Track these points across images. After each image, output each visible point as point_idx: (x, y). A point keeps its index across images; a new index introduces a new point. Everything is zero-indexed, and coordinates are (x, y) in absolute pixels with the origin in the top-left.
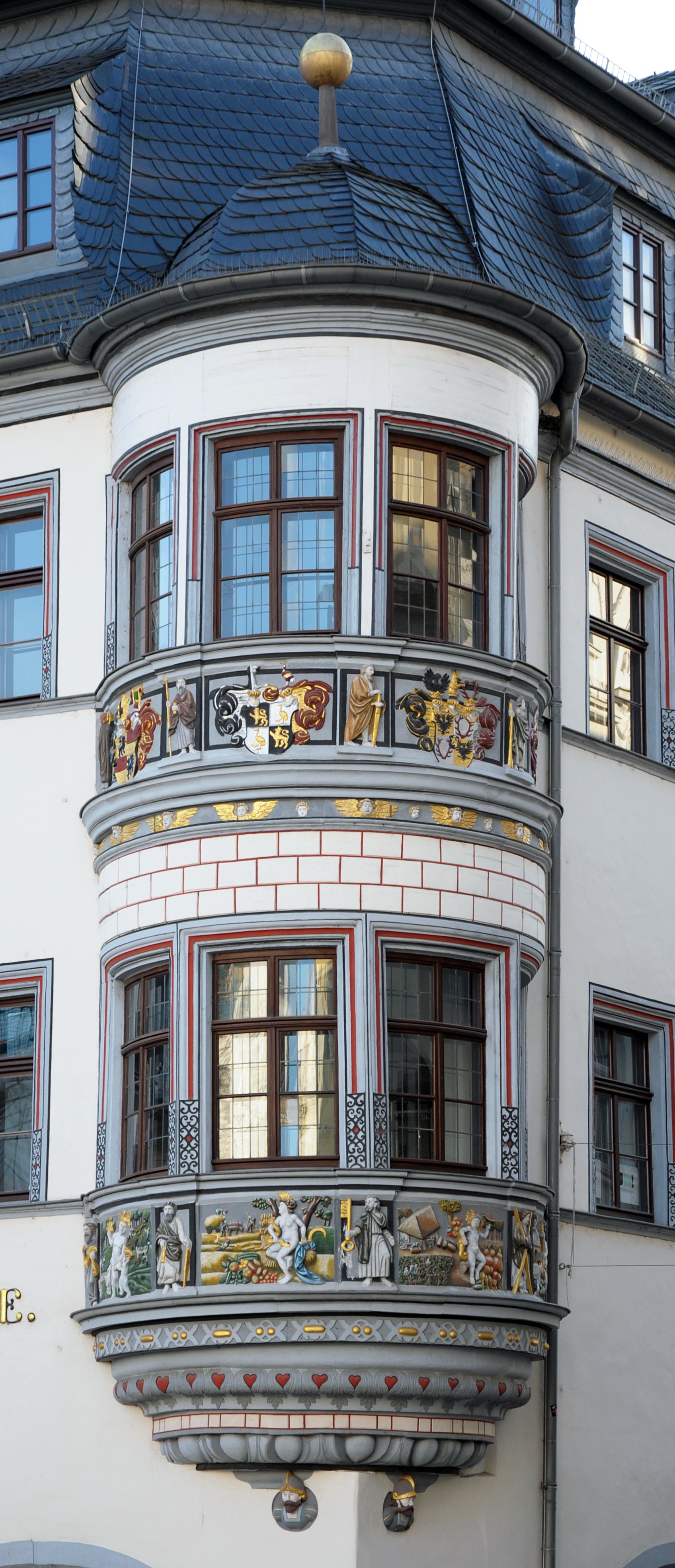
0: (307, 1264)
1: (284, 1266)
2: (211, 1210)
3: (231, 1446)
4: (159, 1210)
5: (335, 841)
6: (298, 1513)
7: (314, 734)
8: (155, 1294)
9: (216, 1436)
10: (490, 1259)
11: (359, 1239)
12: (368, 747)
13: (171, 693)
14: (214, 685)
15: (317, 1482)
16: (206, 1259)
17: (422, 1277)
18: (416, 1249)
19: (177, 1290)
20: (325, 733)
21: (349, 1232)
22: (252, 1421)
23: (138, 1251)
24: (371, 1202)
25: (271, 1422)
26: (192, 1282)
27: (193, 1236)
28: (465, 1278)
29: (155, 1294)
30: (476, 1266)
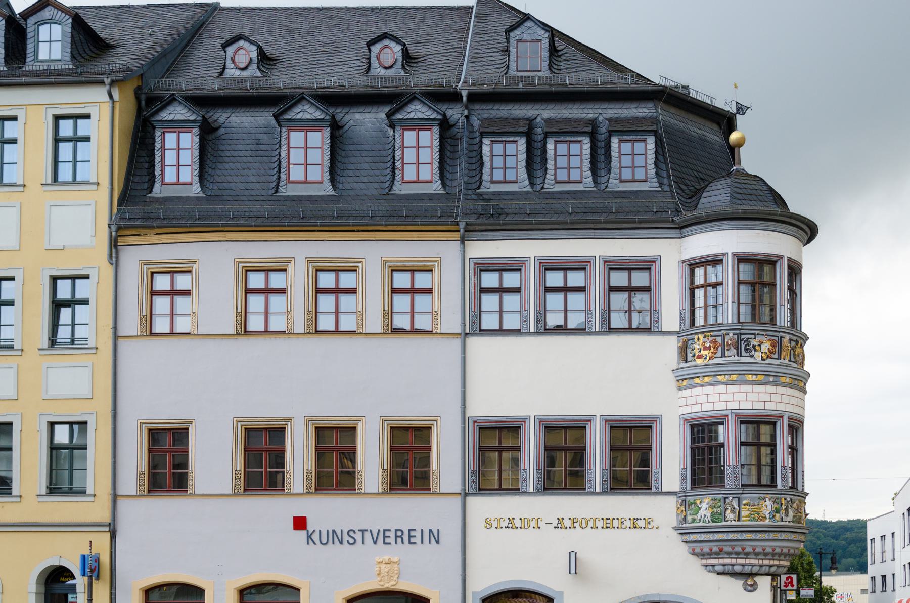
0: (774, 516)
1: (768, 516)
2: (745, 499)
3: (738, 569)
4: (725, 498)
5: (781, 390)
6: (753, 588)
7: (773, 356)
8: (724, 523)
9: (733, 565)
11: (786, 510)
12: (786, 361)
13: (727, 338)
14: (743, 337)
15: (757, 579)
16: (743, 514)
19: (733, 523)
20: (776, 356)
21: (784, 507)
22: (748, 561)
23: (715, 510)
24: (788, 499)
25: (753, 561)
26: (739, 520)
27: (739, 506)
29: (724, 523)
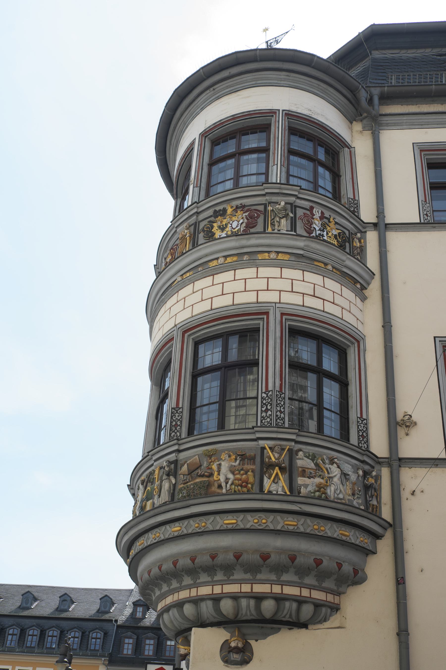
10: (238, 476)
17: (188, 496)
18: (186, 481)
24: (165, 464)
28: (219, 491)
30: (227, 483)
